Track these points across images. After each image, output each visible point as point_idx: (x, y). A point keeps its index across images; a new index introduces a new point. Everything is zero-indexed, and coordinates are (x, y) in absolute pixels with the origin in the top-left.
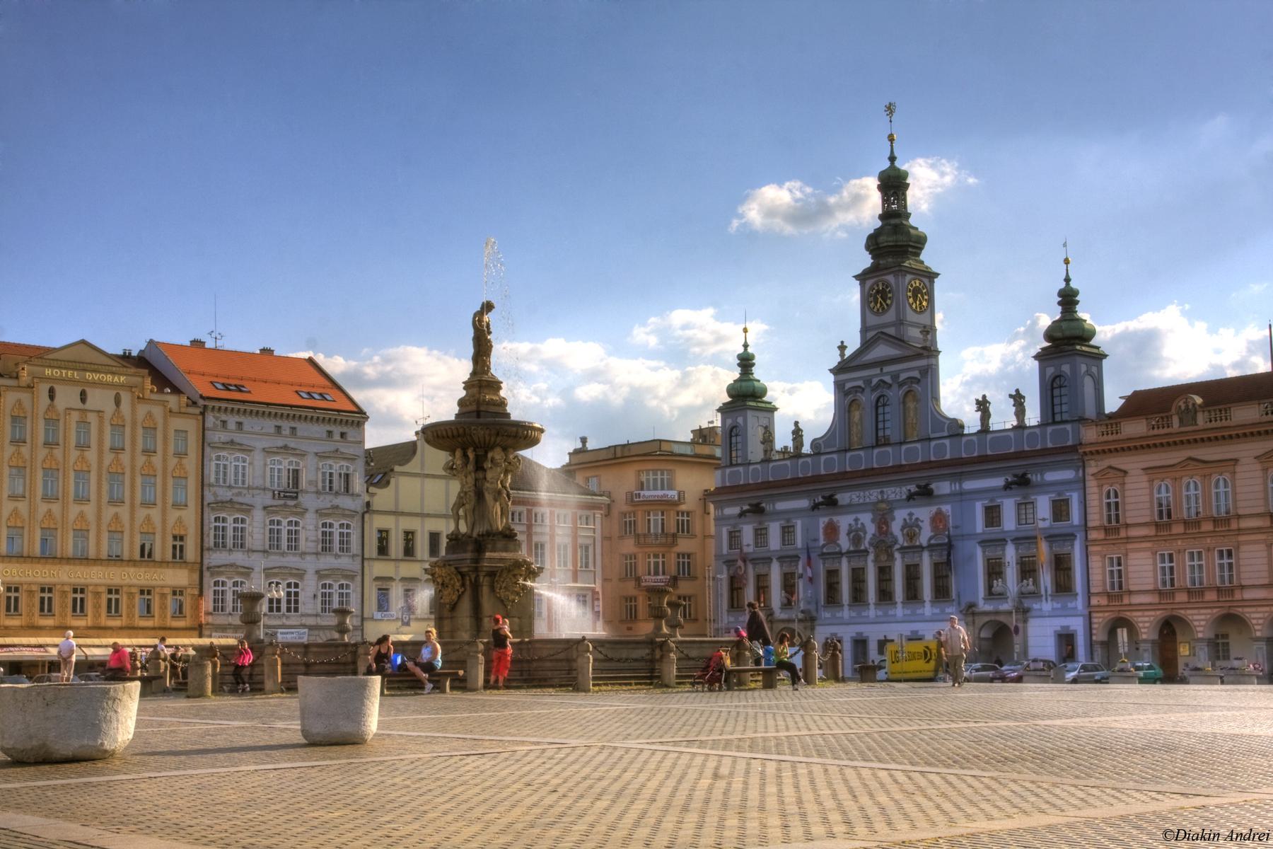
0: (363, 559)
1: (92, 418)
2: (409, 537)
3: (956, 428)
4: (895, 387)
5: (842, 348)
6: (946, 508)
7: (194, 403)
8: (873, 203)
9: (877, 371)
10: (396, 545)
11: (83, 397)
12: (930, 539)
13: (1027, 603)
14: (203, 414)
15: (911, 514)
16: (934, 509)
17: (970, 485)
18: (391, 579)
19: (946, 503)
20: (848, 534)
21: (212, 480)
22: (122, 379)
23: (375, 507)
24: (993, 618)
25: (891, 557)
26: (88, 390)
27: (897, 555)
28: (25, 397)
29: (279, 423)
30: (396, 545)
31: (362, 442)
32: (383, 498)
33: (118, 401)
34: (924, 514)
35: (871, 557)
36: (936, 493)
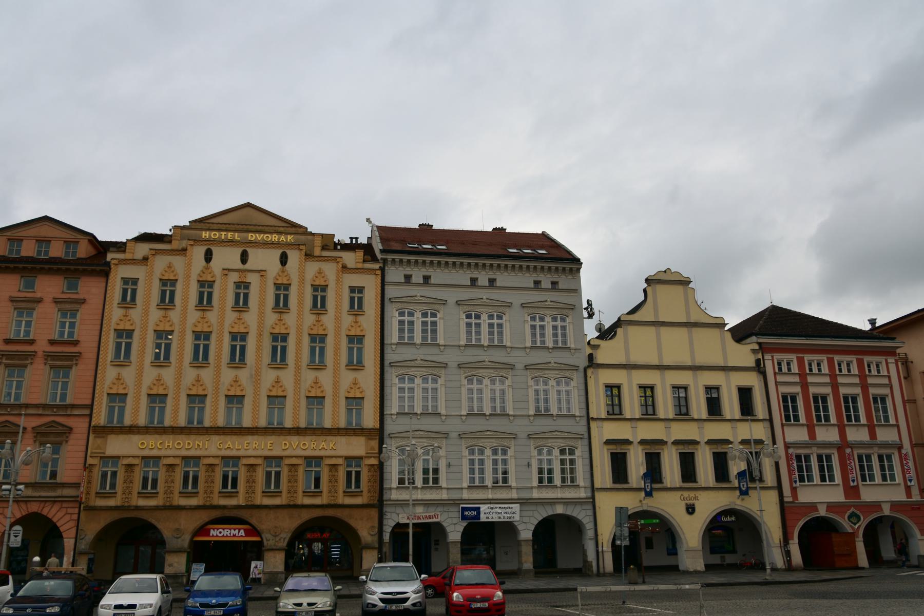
0: (589, 419)
1: (253, 279)
2: (648, 391)
7: (374, 259)
10: (632, 405)
11: (244, 258)
14: (382, 270)
18: (627, 442)
21: (395, 340)
22: (289, 237)
23: (600, 358)
26: (249, 250)
28: (178, 262)
29: (475, 274)
30: (632, 405)
31: (577, 291)
32: (608, 352)
33: (284, 259)
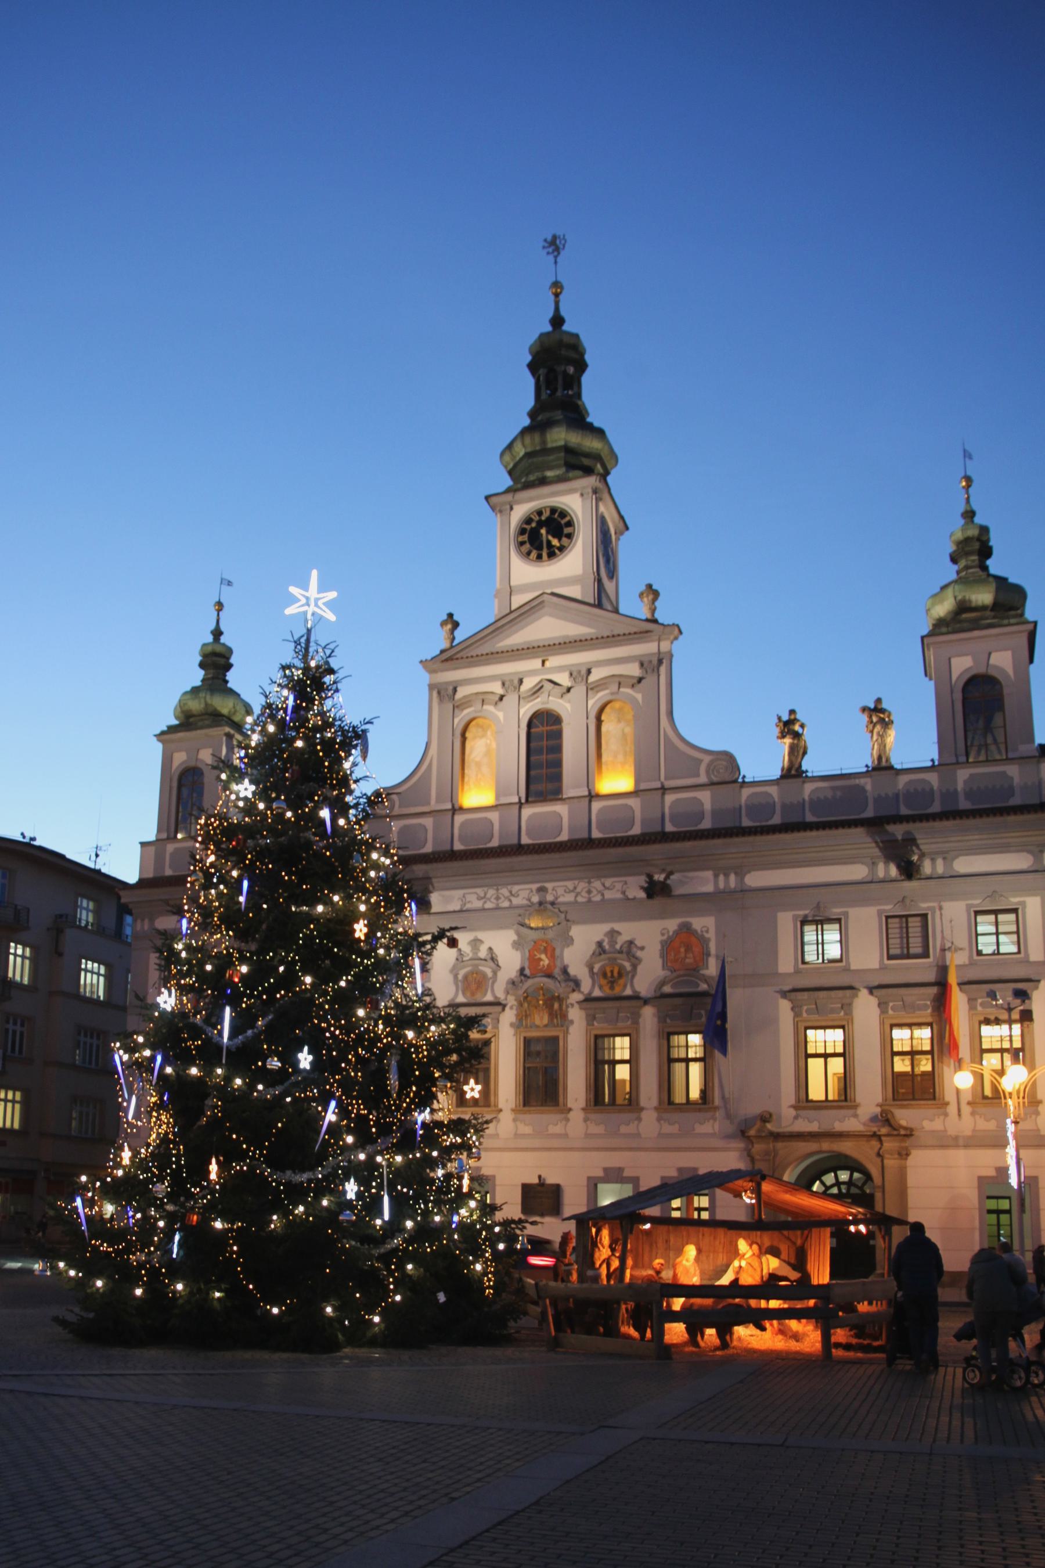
3: (725, 769)
4: (579, 691)
5: (452, 622)
6: (704, 923)
8: (521, 394)
9: (536, 663)
12: (663, 983)
13: (904, 1116)
15: (613, 934)
16: (672, 925)
17: (756, 879)
19: (701, 913)
20: (454, 971)
24: (826, 1145)
25: (559, 1017)
27: (576, 1014)
34: (648, 934)
35: (508, 1016)
36: (678, 891)
